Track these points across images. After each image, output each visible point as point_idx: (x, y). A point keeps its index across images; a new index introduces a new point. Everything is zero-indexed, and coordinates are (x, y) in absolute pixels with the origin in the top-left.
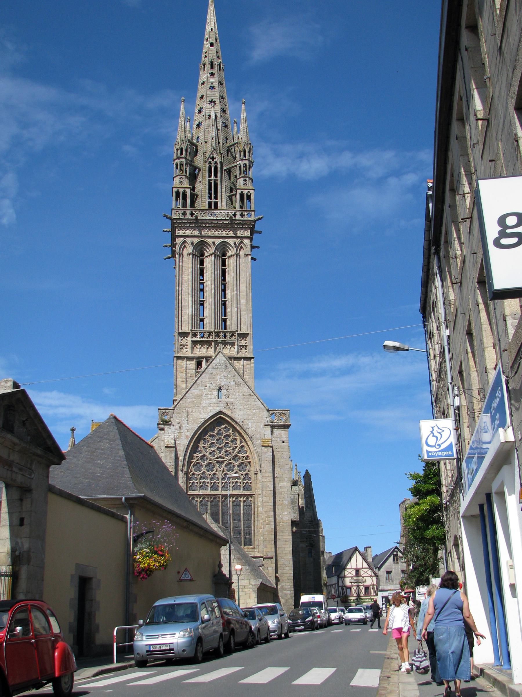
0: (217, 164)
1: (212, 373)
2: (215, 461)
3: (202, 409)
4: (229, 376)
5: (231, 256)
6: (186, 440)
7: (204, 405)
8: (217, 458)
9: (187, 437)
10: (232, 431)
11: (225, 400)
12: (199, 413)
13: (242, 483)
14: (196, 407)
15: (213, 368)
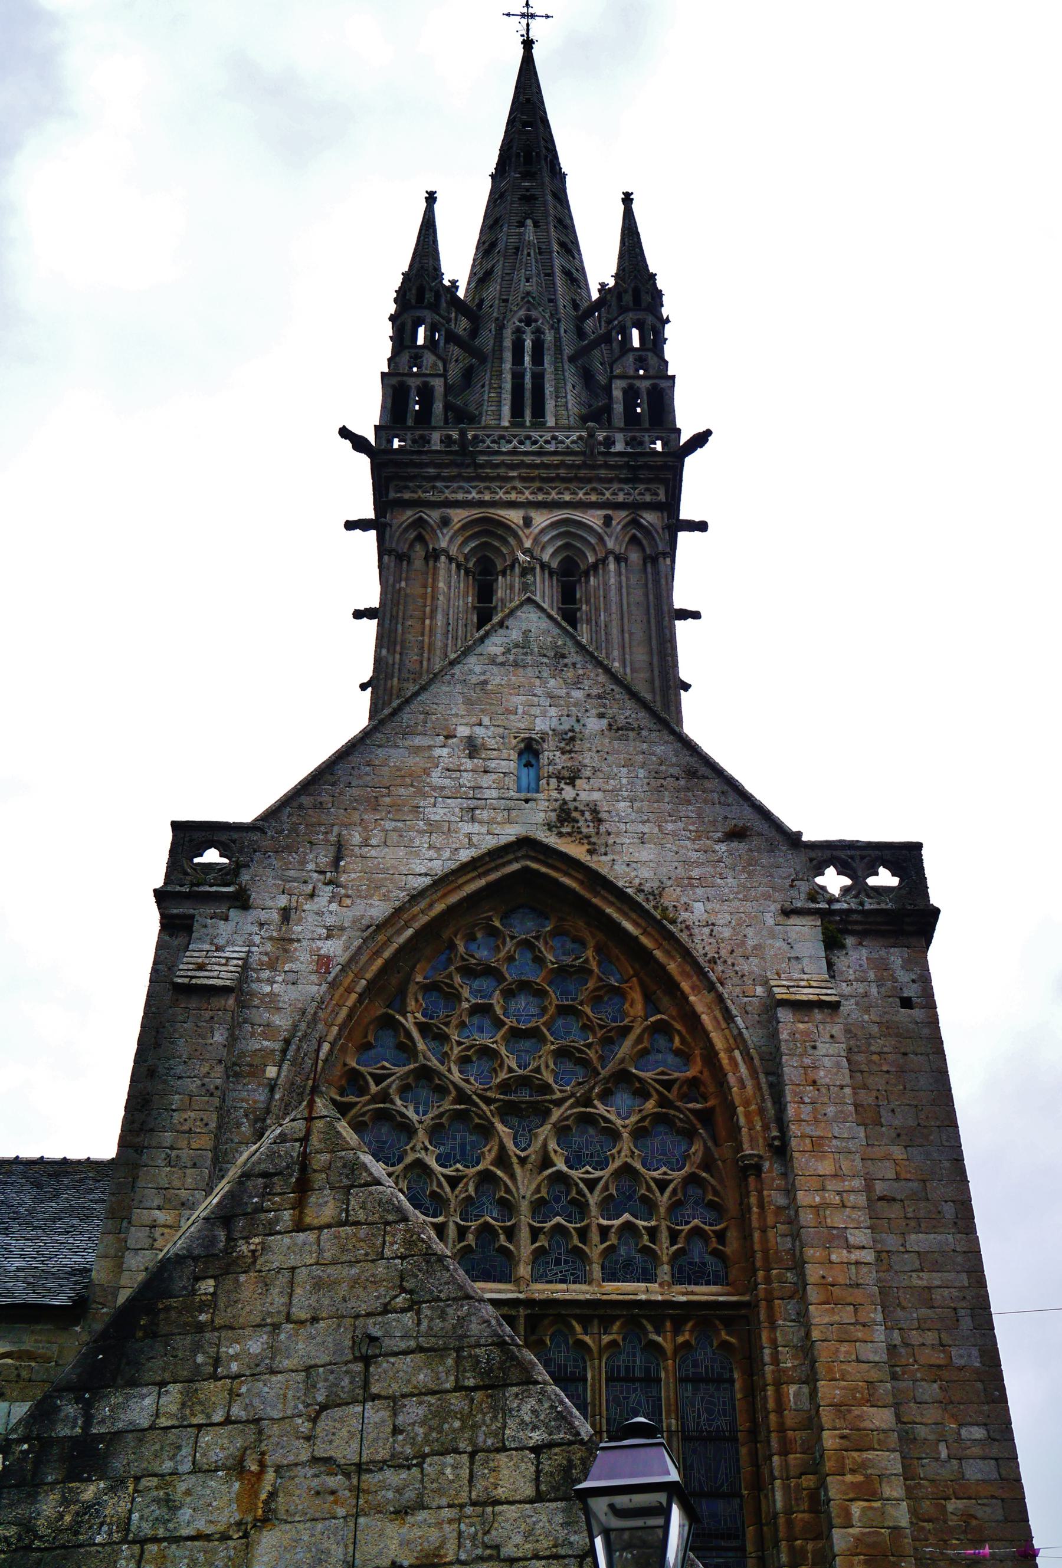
0: (543, 333)
1: (485, 682)
2: (488, 1101)
3: (421, 832)
4: (578, 694)
5: (595, 567)
6: (314, 978)
7: (437, 813)
8: (504, 1087)
9: (323, 962)
10: (599, 950)
11: (555, 794)
12: (401, 852)
13: (664, 1236)
14: (389, 825)
15: (492, 661)
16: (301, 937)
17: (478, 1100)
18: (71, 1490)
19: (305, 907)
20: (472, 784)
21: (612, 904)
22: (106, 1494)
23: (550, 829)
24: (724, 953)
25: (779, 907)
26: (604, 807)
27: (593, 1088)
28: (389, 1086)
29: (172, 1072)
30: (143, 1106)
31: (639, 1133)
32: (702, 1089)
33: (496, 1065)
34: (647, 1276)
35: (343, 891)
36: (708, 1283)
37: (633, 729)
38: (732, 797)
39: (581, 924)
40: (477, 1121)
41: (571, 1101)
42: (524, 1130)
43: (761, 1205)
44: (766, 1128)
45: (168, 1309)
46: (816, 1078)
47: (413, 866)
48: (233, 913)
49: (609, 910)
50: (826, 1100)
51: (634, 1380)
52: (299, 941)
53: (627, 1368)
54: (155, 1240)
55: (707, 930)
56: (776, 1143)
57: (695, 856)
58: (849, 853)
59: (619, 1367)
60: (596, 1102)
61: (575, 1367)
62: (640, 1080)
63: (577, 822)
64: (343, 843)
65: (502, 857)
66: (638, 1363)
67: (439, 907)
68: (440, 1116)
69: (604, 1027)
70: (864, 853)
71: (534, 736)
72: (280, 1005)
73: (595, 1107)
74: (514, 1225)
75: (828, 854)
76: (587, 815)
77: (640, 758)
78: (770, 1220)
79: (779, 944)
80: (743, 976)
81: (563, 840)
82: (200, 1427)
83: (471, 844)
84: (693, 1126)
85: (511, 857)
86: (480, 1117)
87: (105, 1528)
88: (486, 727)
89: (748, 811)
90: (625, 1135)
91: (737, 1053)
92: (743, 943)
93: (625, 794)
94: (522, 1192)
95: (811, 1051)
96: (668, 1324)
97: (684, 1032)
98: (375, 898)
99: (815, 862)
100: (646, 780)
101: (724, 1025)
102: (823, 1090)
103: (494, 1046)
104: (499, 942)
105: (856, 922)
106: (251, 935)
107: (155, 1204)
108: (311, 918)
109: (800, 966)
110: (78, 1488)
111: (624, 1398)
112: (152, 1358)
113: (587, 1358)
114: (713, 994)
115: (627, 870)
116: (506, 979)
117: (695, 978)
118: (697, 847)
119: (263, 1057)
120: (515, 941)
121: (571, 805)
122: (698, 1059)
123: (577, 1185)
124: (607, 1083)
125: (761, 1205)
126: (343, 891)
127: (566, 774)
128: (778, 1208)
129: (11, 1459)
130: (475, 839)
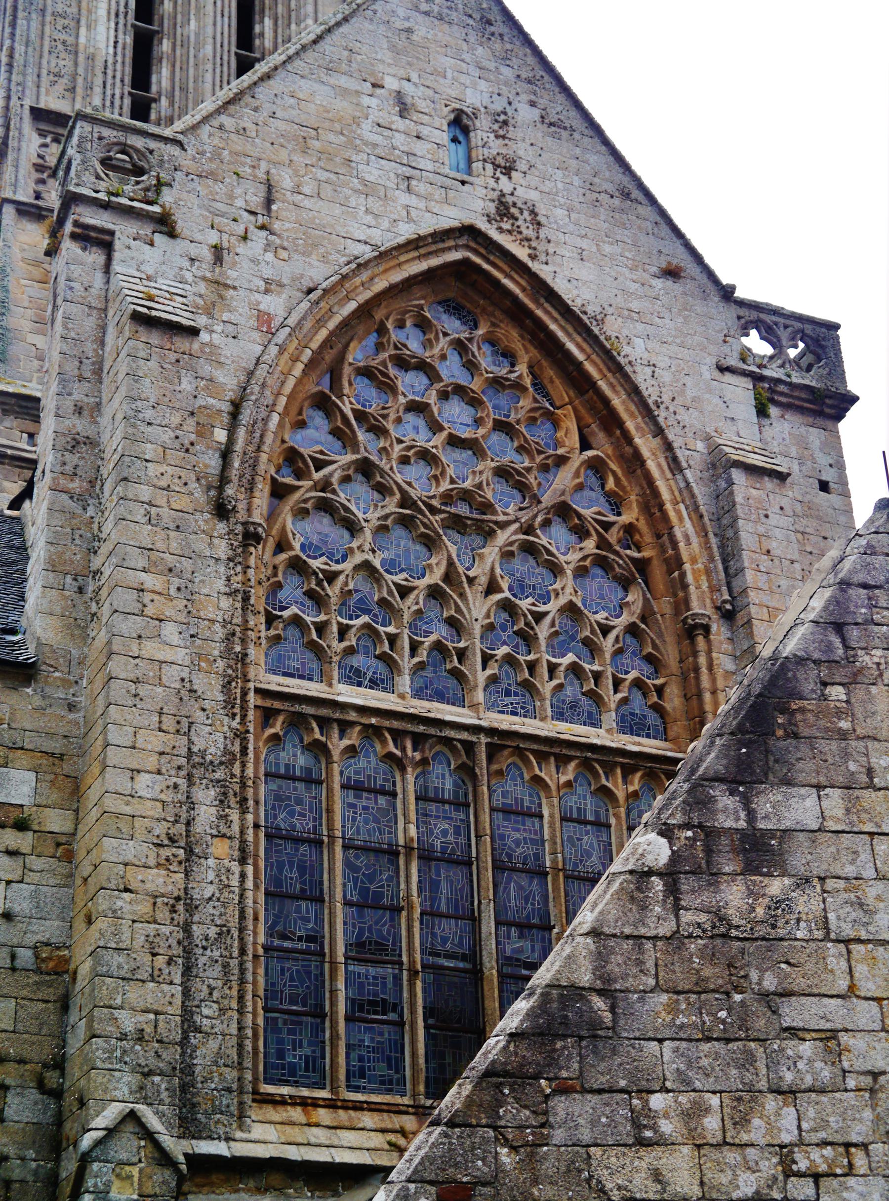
1: (409, 31)
2: (433, 510)
7: (373, 172)
9: (264, 319)
11: (492, 183)
16: (236, 284)
17: (423, 507)
18: (754, 883)
19: (238, 250)
20: (406, 149)
21: (556, 320)
22: (793, 891)
23: (489, 221)
24: (666, 398)
25: (714, 361)
26: (541, 210)
27: (536, 516)
28: (331, 475)
29: (141, 416)
30: (73, 447)
31: (581, 572)
32: (637, 537)
33: (438, 473)
34: (594, 722)
35: (278, 241)
36: (648, 736)
37: (565, 128)
38: (665, 230)
39: (514, 334)
40: (423, 530)
41: (516, 526)
42: (466, 548)
43: (710, 667)
44: (713, 589)
45: (802, 710)
46: (770, 548)
47: (351, 229)
48: (158, 238)
49: (553, 327)
50: (779, 572)
51: (586, 823)
52: (235, 288)
53: (579, 809)
54: (145, 606)
55: (648, 371)
56: (728, 607)
57: (634, 287)
58: (774, 318)
59: (571, 807)
60: (538, 531)
61: (532, 802)
62: (579, 516)
63: (517, 219)
64: (272, 183)
65: (443, 241)
66: (589, 807)
67: (380, 285)
68: (386, 517)
69: (542, 452)
70: (788, 322)
71: (465, 109)
72: (222, 360)
73: (538, 537)
74: (466, 648)
75: (754, 315)
76: (526, 213)
77: (574, 163)
78: (720, 684)
79: (716, 400)
80: (684, 427)
81: (503, 235)
82: (871, 834)
83: (409, 219)
84: (633, 575)
85: (451, 243)
86: (425, 526)
87: (803, 924)
88: (415, 84)
89: (681, 251)
90: (569, 572)
91: (682, 507)
92: (682, 393)
93: (562, 201)
94: (475, 614)
95: (764, 520)
96: (619, 771)
97: (619, 472)
98: (314, 257)
99: (743, 321)
100: (582, 191)
101: (669, 476)
102: (776, 561)
103: (434, 450)
104: (432, 336)
105: (782, 394)
106: (181, 269)
107: (140, 566)
108: (246, 264)
109: (735, 428)
110: (761, 882)
111: (579, 839)
112: (801, 759)
113: (542, 794)
114: (658, 439)
115: (569, 286)
116: (441, 380)
117: (639, 419)
118: (635, 277)
119: (209, 416)
120: (448, 338)
121: (510, 199)
122: (634, 505)
123: (525, 616)
124: (548, 513)
125: (710, 667)
126: (278, 241)
127: (500, 161)
128: (727, 672)
129: (678, 845)
130: (414, 214)
